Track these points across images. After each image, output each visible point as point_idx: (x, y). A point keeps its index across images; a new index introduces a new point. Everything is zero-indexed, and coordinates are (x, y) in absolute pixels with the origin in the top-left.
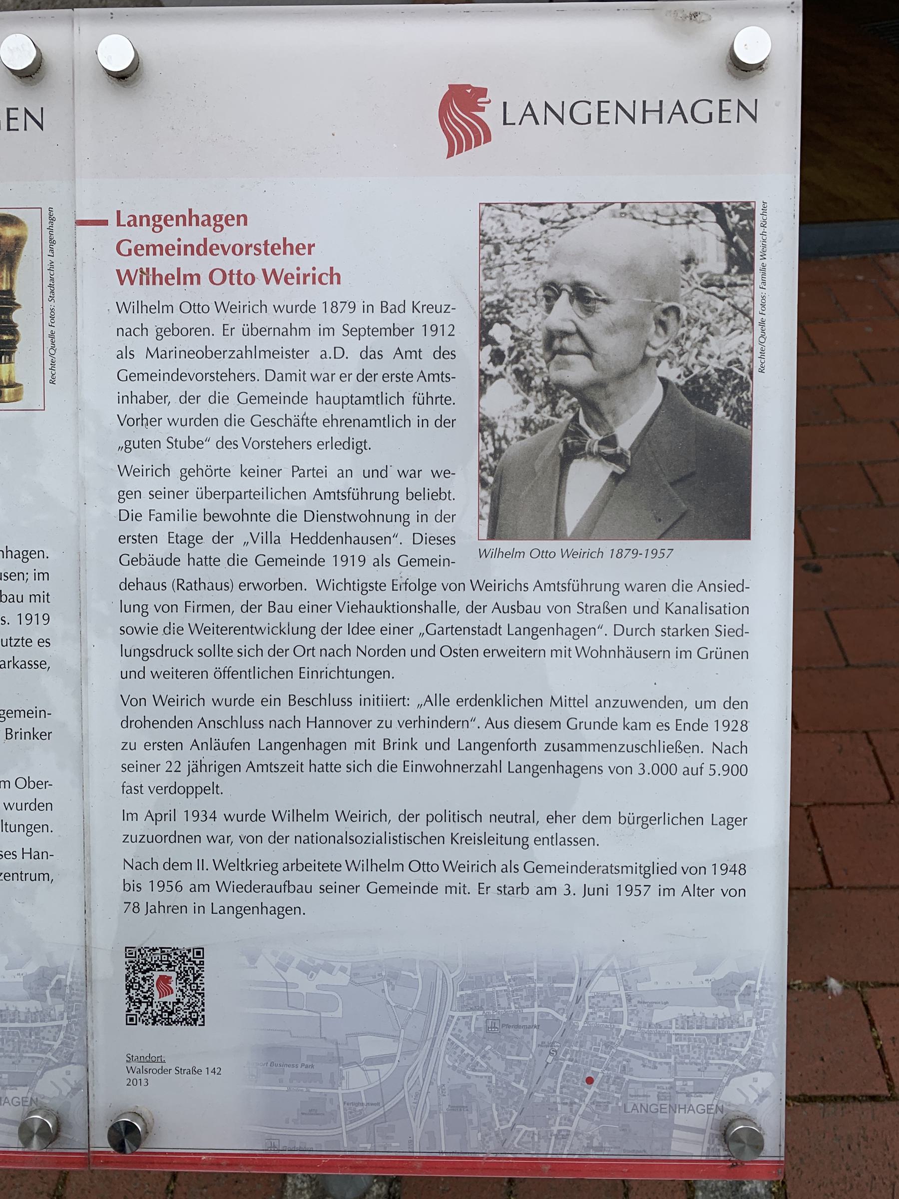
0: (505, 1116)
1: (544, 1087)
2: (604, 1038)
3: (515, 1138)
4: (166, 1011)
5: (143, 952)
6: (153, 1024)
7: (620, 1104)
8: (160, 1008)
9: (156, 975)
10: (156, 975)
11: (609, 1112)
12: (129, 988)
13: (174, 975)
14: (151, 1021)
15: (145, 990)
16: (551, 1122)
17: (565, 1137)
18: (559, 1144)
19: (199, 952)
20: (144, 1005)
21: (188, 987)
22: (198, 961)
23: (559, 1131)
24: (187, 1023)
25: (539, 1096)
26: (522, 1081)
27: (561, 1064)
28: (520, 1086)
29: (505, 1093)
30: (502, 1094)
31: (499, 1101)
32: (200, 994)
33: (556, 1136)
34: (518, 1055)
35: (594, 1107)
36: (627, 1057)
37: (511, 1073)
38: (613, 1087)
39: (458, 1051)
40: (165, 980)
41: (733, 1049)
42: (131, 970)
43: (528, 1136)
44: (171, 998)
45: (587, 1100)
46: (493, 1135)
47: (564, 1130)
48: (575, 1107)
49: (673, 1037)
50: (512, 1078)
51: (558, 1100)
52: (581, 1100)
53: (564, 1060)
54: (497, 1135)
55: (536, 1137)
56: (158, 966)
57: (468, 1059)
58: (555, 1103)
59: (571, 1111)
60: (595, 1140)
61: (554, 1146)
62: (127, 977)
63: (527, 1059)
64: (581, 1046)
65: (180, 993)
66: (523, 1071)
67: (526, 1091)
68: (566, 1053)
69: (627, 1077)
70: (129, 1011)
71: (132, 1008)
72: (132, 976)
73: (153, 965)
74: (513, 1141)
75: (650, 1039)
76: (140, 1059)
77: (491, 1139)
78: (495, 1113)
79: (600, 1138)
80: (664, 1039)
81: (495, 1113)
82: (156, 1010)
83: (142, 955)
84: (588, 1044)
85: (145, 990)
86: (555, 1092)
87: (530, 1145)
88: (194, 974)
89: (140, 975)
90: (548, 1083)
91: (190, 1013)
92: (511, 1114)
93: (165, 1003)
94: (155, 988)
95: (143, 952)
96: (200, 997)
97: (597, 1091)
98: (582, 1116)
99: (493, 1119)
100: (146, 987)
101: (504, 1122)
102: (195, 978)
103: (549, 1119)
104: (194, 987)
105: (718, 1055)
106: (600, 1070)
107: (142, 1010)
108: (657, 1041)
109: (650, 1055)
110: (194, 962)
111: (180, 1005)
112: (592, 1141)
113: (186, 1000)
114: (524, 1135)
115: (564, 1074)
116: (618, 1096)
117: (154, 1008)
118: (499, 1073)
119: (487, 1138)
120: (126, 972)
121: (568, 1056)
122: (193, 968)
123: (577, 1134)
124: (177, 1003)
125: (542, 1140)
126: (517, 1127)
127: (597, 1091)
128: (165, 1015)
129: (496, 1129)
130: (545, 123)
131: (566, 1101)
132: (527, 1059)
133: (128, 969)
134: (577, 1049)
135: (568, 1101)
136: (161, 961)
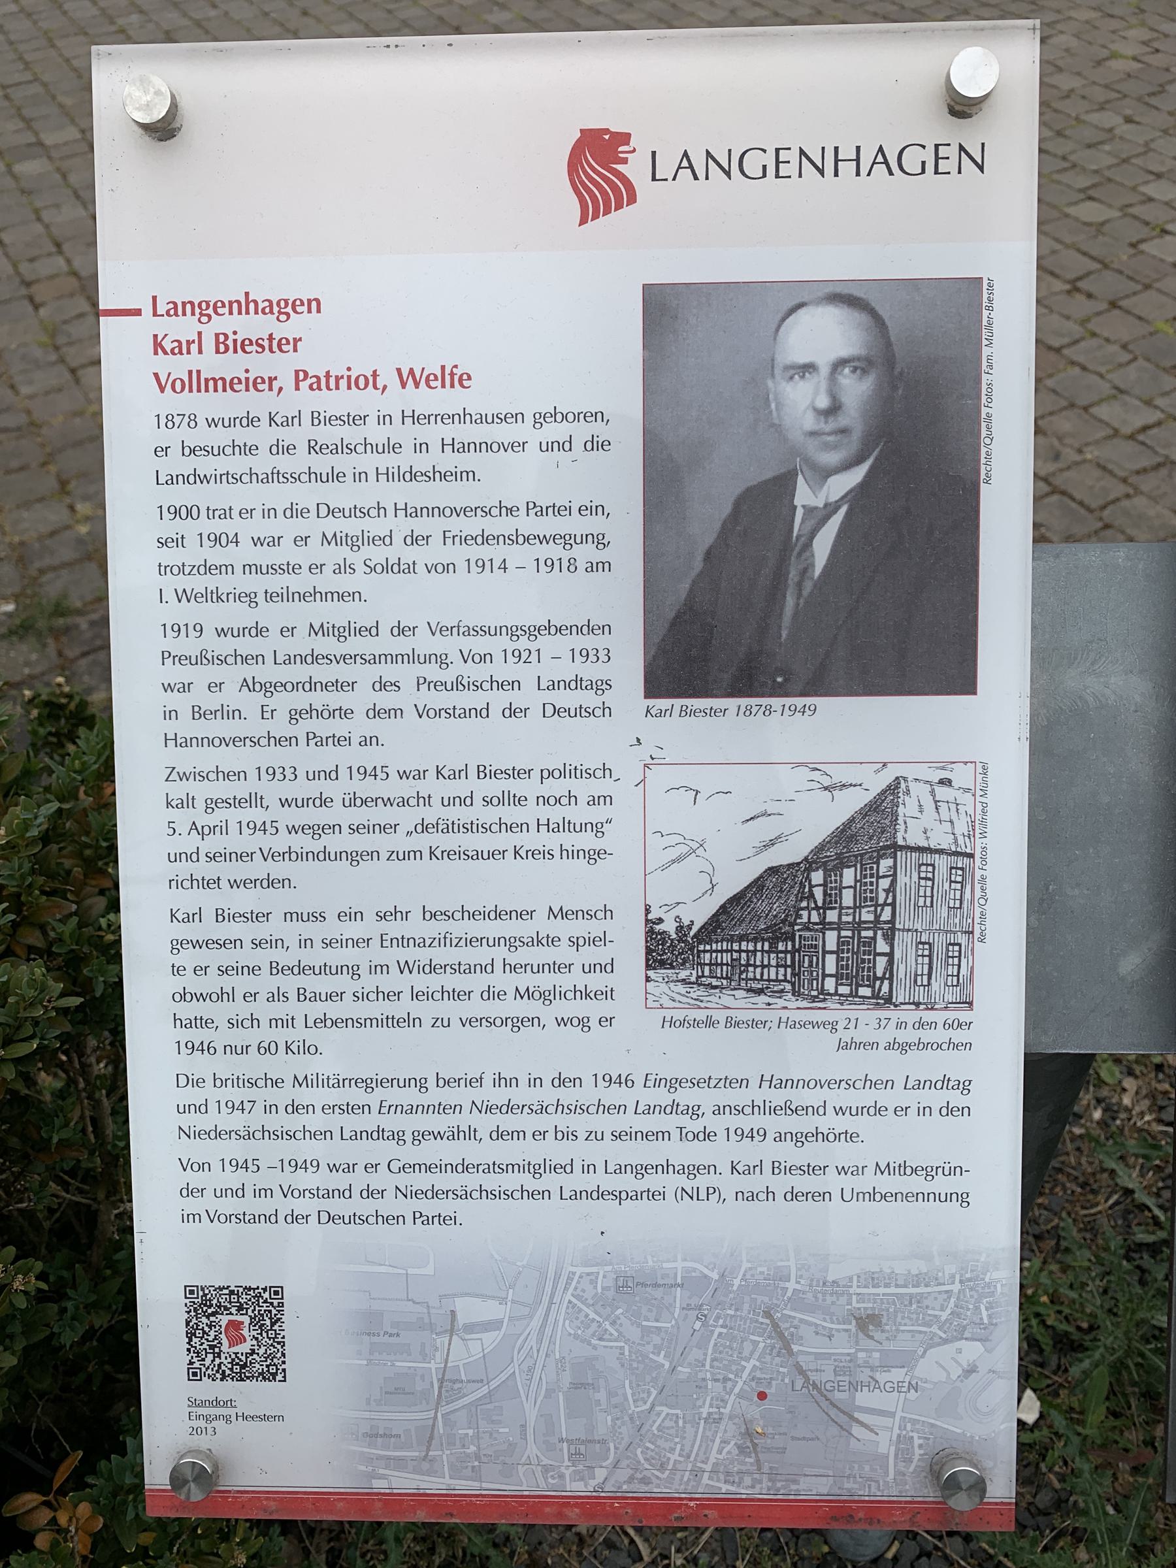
0: (642, 1395)
2: (766, 1299)
3: (654, 1422)
4: (237, 1364)
5: (207, 1291)
6: (222, 1380)
7: (787, 1381)
8: (229, 1360)
9: (224, 1319)
10: (224, 1319)
12: (190, 1336)
13: (246, 1320)
14: (218, 1376)
15: (210, 1339)
16: (699, 1403)
17: (718, 1421)
19: (278, 1291)
20: (210, 1357)
21: (264, 1335)
22: (275, 1302)
23: (710, 1414)
24: (264, 1378)
25: (684, 1370)
26: (663, 1353)
27: (712, 1332)
28: (660, 1359)
29: (641, 1366)
30: (637, 1369)
32: (279, 1343)
34: (657, 1321)
35: (753, 1384)
36: (796, 1322)
37: (648, 1343)
39: (583, 1314)
40: (235, 1326)
41: (930, 1312)
42: (193, 1314)
44: (244, 1348)
45: (745, 1375)
46: (626, 1418)
48: (729, 1385)
49: (854, 1297)
50: (650, 1348)
51: (709, 1375)
52: (736, 1376)
53: (716, 1326)
54: (631, 1419)
55: (681, 1423)
56: (226, 1308)
57: (595, 1325)
58: (704, 1380)
59: (725, 1387)
62: (187, 1323)
63: (669, 1325)
64: (737, 1310)
65: (255, 1342)
66: (663, 1339)
68: (718, 1318)
70: (191, 1363)
71: (195, 1360)
72: (194, 1321)
73: (219, 1307)
74: (652, 1426)
75: (824, 1300)
76: (203, 1404)
77: (623, 1424)
78: (629, 1392)
80: (843, 1300)
82: (225, 1362)
83: (205, 1295)
84: (746, 1307)
85: (210, 1339)
86: (704, 1365)
87: (672, 1431)
88: (271, 1318)
89: (204, 1320)
90: (695, 1354)
91: (267, 1366)
92: (649, 1393)
93: (236, 1354)
94: (223, 1336)
95: (207, 1291)
96: (279, 1347)
97: (758, 1364)
98: (739, 1396)
99: (626, 1399)
100: (212, 1334)
101: (640, 1403)
102: (273, 1324)
103: (697, 1399)
104: (272, 1334)
105: (911, 1319)
106: (761, 1339)
107: (208, 1362)
108: (833, 1303)
109: (825, 1320)
110: (272, 1304)
111: (255, 1356)
113: (262, 1351)
115: (716, 1345)
116: (785, 1370)
117: (223, 1360)
118: (634, 1343)
119: (618, 1423)
120: (186, 1316)
121: (721, 1322)
122: (270, 1312)
124: (251, 1354)
126: (658, 1408)
127: (758, 1364)
128: (237, 1369)
130: (707, 178)
131: (719, 1377)
132: (669, 1325)
133: (188, 1312)
134: (731, 1312)
135: (721, 1377)
136: (230, 1302)
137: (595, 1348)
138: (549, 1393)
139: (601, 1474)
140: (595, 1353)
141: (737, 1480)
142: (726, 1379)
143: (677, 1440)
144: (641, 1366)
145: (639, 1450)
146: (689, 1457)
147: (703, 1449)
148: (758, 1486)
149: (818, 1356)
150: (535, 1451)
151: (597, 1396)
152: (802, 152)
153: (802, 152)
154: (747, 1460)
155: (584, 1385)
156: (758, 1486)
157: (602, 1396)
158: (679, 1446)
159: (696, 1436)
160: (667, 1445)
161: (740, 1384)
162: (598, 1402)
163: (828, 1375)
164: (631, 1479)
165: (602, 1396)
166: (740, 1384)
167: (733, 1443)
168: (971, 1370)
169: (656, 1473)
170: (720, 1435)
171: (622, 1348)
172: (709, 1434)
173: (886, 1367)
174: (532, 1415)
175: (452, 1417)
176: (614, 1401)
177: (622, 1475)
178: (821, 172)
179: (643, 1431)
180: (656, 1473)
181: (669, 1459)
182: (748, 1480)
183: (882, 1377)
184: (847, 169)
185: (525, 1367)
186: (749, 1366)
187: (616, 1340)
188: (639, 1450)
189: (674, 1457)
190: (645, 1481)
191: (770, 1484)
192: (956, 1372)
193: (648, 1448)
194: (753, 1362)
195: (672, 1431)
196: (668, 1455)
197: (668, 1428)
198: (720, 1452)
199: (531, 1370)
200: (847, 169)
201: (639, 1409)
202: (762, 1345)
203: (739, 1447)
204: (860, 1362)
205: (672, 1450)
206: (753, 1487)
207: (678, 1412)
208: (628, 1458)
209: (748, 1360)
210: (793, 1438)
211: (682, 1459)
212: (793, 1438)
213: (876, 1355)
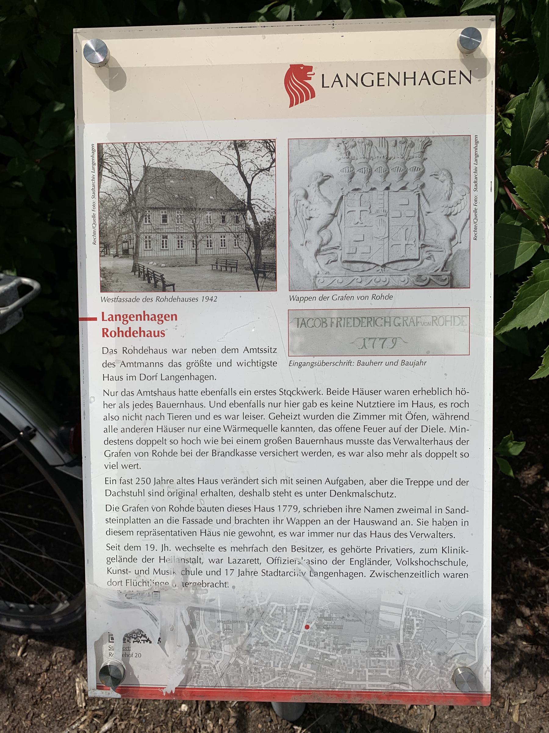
3: (270, 611)
17: (305, 610)
18: (301, 616)
23: (301, 606)
33: (299, 610)
43: (279, 610)
47: (304, 606)
55: (285, 611)
60: (325, 612)
61: (297, 617)
74: (268, 613)
79: (329, 611)
87: (280, 617)
112: (323, 614)
114: (276, 609)
123: (312, 609)
129: (257, 605)
141: (316, 644)
143: (282, 621)
145: (262, 627)
147: (297, 627)
148: (328, 647)
154: (322, 632)
156: (328, 647)
158: (284, 625)
159: (293, 619)
160: (277, 624)
164: (257, 643)
167: (313, 623)
169: (272, 640)
170: (306, 618)
172: (300, 618)
179: (264, 616)
180: (272, 640)
181: (278, 632)
182: (322, 644)
188: (262, 627)
190: (265, 644)
191: (334, 646)
193: (267, 626)
196: (278, 630)
197: (278, 614)
201: (261, 604)
206: (325, 648)
207: (283, 605)
210: (347, 620)
211: (285, 632)
212: (347, 620)
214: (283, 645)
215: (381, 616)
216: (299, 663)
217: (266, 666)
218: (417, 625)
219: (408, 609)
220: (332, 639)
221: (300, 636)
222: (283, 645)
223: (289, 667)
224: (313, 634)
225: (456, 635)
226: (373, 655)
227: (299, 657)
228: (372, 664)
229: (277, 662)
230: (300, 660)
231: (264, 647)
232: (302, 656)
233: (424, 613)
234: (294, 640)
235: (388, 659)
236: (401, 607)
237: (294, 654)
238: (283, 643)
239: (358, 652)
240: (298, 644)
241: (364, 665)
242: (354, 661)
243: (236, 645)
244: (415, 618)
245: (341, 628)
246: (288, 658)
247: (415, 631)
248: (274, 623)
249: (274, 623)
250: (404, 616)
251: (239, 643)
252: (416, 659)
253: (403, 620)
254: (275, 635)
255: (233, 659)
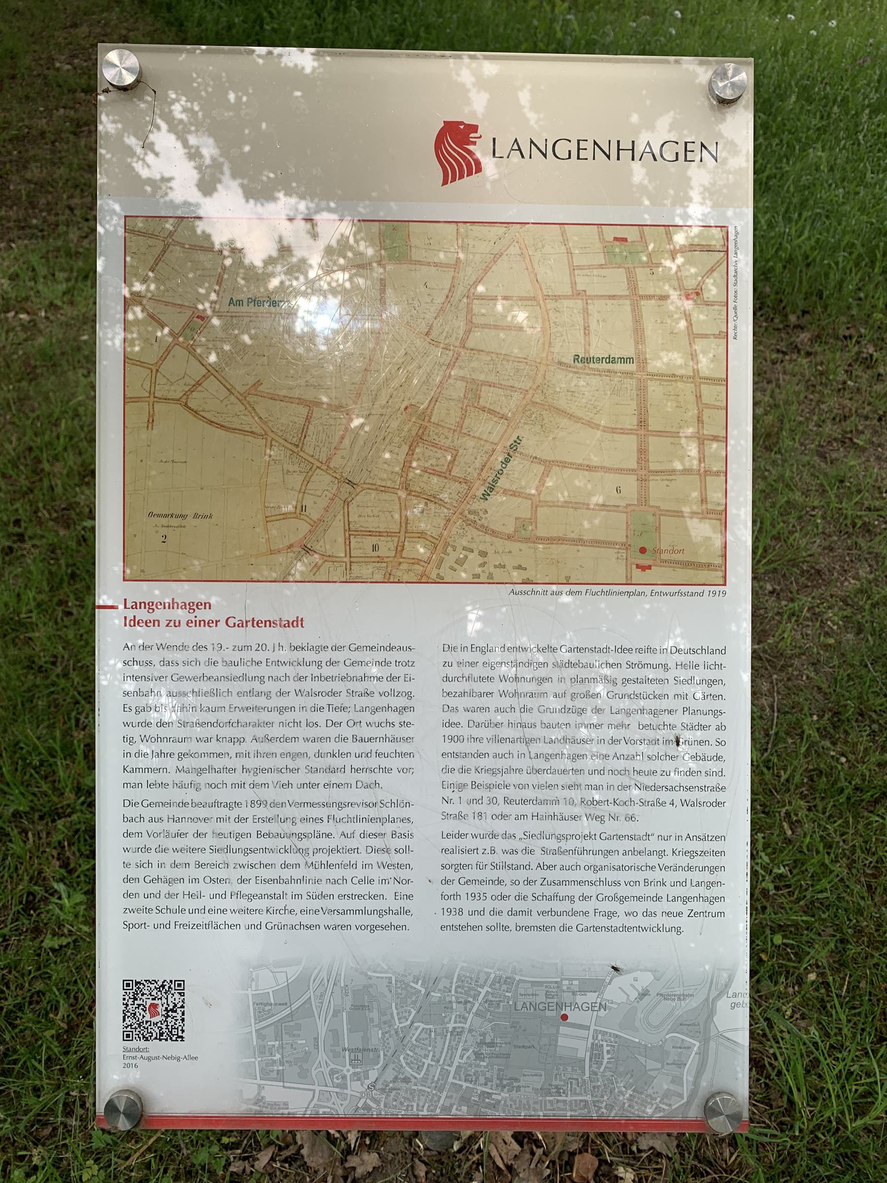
1: (441, 987)
11: (501, 1010)
16: (446, 1020)
17: (460, 1034)
23: (454, 1028)
28: (418, 987)
29: (404, 992)
31: (398, 1001)
38: (504, 987)
46: (393, 1032)
48: (469, 1006)
52: (474, 999)
54: (396, 1032)
67: (423, 991)
69: (517, 978)
77: (390, 1036)
78: (395, 1012)
81: (395, 1012)
87: (427, 1042)
92: (410, 1012)
98: (476, 1014)
99: (393, 1018)
123: (470, 1031)
125: (439, 1038)
137: (370, 978)
138: (336, 1013)
139: (373, 1075)
140: (370, 982)
142: (466, 1002)
144: (404, 992)
146: (438, 1061)
149: (533, 983)
150: (325, 1057)
151: (371, 1015)
152: (595, 143)
153: (595, 143)
155: (363, 1007)
157: (375, 1015)
160: (423, 1053)
161: (477, 1005)
162: (372, 1020)
163: (541, 998)
164: (396, 1078)
165: (375, 1015)
166: (477, 1005)
168: (644, 994)
171: (390, 978)
172: (453, 1043)
173: (583, 992)
174: (322, 1029)
175: (263, 1032)
176: (384, 1019)
177: (390, 1075)
178: (608, 157)
179: (405, 1042)
182: (482, 1080)
183: (580, 999)
184: (626, 155)
185: (318, 993)
186: (483, 992)
187: (386, 972)
189: (427, 1061)
190: (406, 1080)
192: (634, 995)
194: (486, 988)
195: (427, 1042)
198: (462, 1057)
199: (322, 995)
200: (626, 155)
202: (492, 976)
203: (475, 1053)
204: (565, 988)
205: (426, 1056)
206: (486, 1084)
208: (394, 1062)
209: (482, 987)
213: (576, 982)
214: (429, 1081)
215: (561, 1041)
216: (451, 1106)
217: (407, 1110)
218: (608, 1052)
219: (596, 1031)
220: (495, 1072)
221: (453, 1070)
222: (429, 1081)
223: (438, 1111)
224: (470, 1065)
225: (659, 1066)
226: (549, 1093)
227: (451, 1097)
228: (549, 1106)
229: (421, 1104)
230: (453, 1101)
231: (404, 1085)
232: (455, 1095)
233: (617, 1036)
234: (445, 1074)
235: (569, 1099)
236: (587, 1028)
237: (445, 1093)
238: (430, 1077)
239: (530, 1090)
240: (450, 1080)
241: (537, 1107)
242: (524, 1102)
243: (367, 1082)
244: (605, 1044)
245: (508, 1056)
246: (436, 1098)
247: (605, 1061)
248: (417, 1050)
249: (417, 1050)
250: (590, 1040)
251: (372, 1078)
252: (606, 1098)
253: (589, 1045)
254: (419, 1069)
255: (363, 1101)
